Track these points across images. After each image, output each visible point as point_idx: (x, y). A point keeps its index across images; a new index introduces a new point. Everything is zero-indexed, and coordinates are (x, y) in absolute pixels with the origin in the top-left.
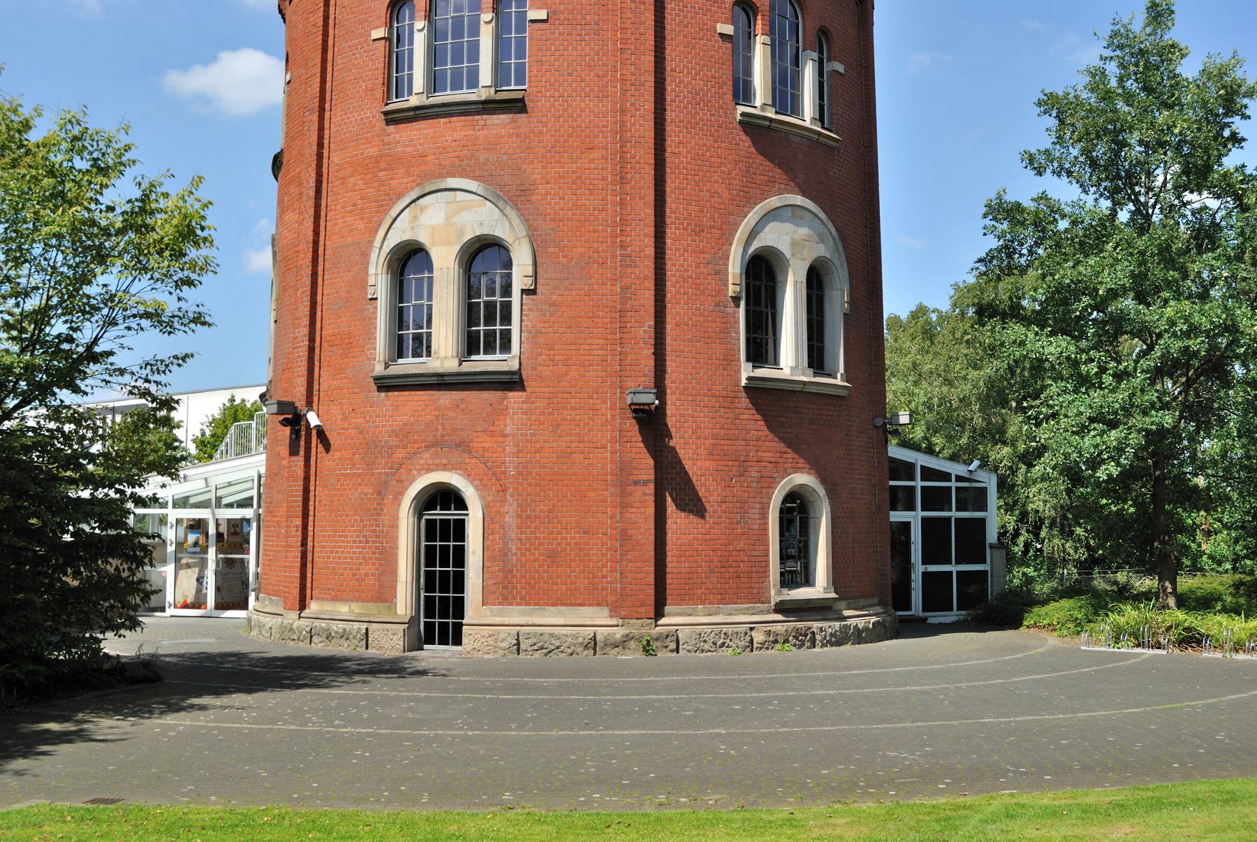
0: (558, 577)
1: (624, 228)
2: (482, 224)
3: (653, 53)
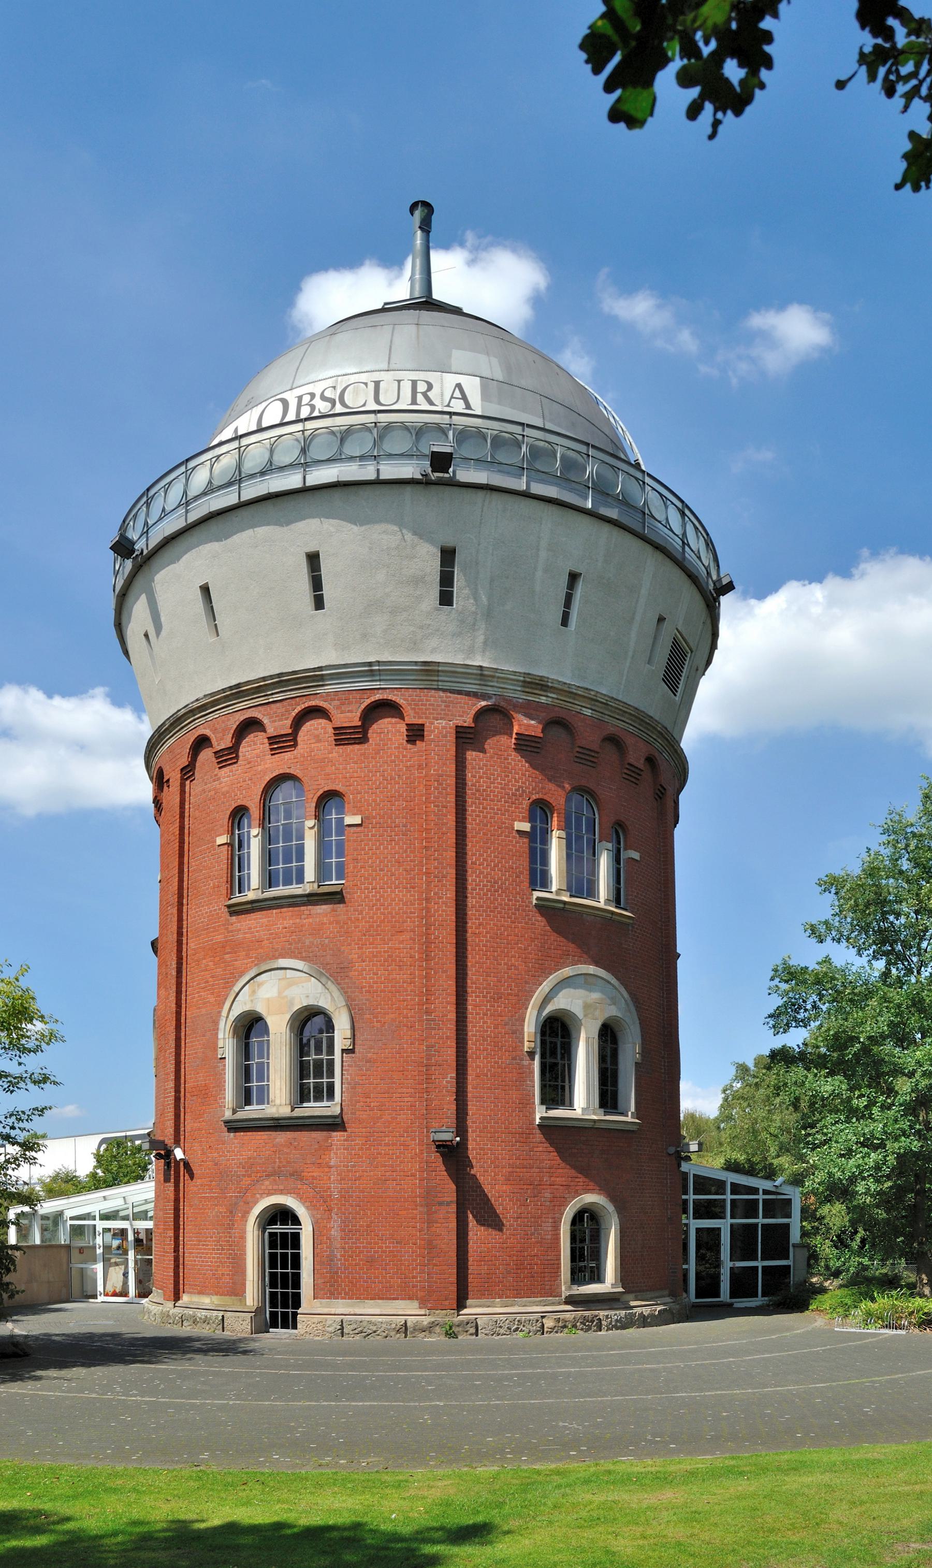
0: (375, 1277)
1: (429, 997)
2: (308, 996)
3: (454, 850)
